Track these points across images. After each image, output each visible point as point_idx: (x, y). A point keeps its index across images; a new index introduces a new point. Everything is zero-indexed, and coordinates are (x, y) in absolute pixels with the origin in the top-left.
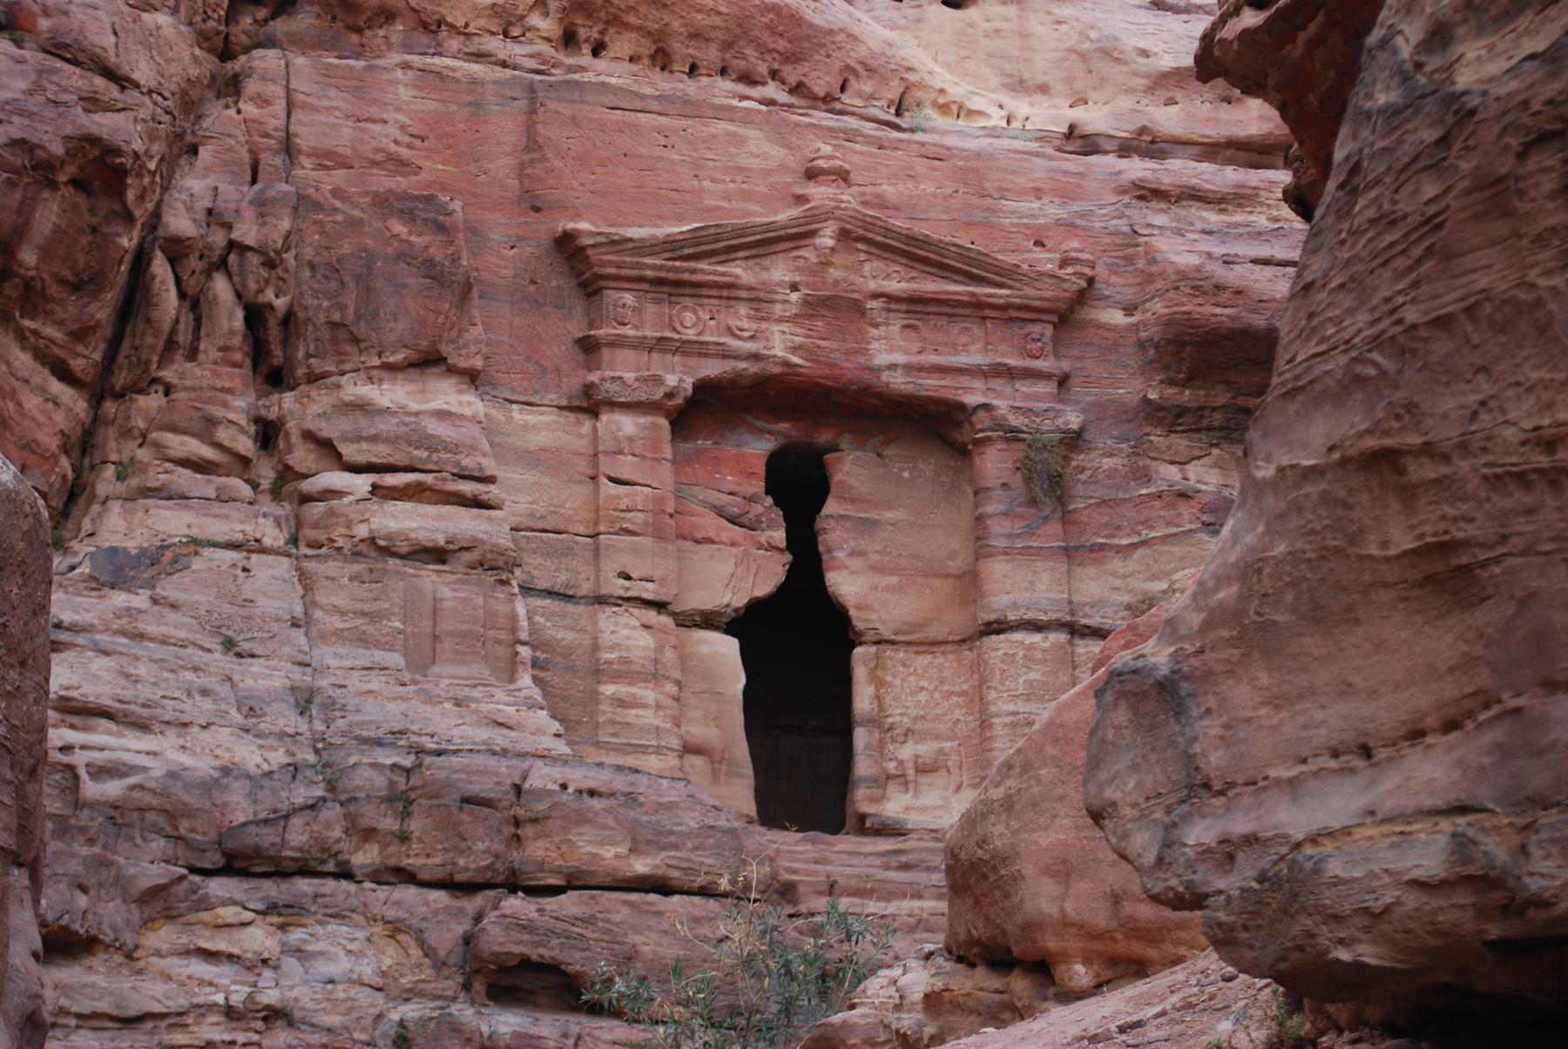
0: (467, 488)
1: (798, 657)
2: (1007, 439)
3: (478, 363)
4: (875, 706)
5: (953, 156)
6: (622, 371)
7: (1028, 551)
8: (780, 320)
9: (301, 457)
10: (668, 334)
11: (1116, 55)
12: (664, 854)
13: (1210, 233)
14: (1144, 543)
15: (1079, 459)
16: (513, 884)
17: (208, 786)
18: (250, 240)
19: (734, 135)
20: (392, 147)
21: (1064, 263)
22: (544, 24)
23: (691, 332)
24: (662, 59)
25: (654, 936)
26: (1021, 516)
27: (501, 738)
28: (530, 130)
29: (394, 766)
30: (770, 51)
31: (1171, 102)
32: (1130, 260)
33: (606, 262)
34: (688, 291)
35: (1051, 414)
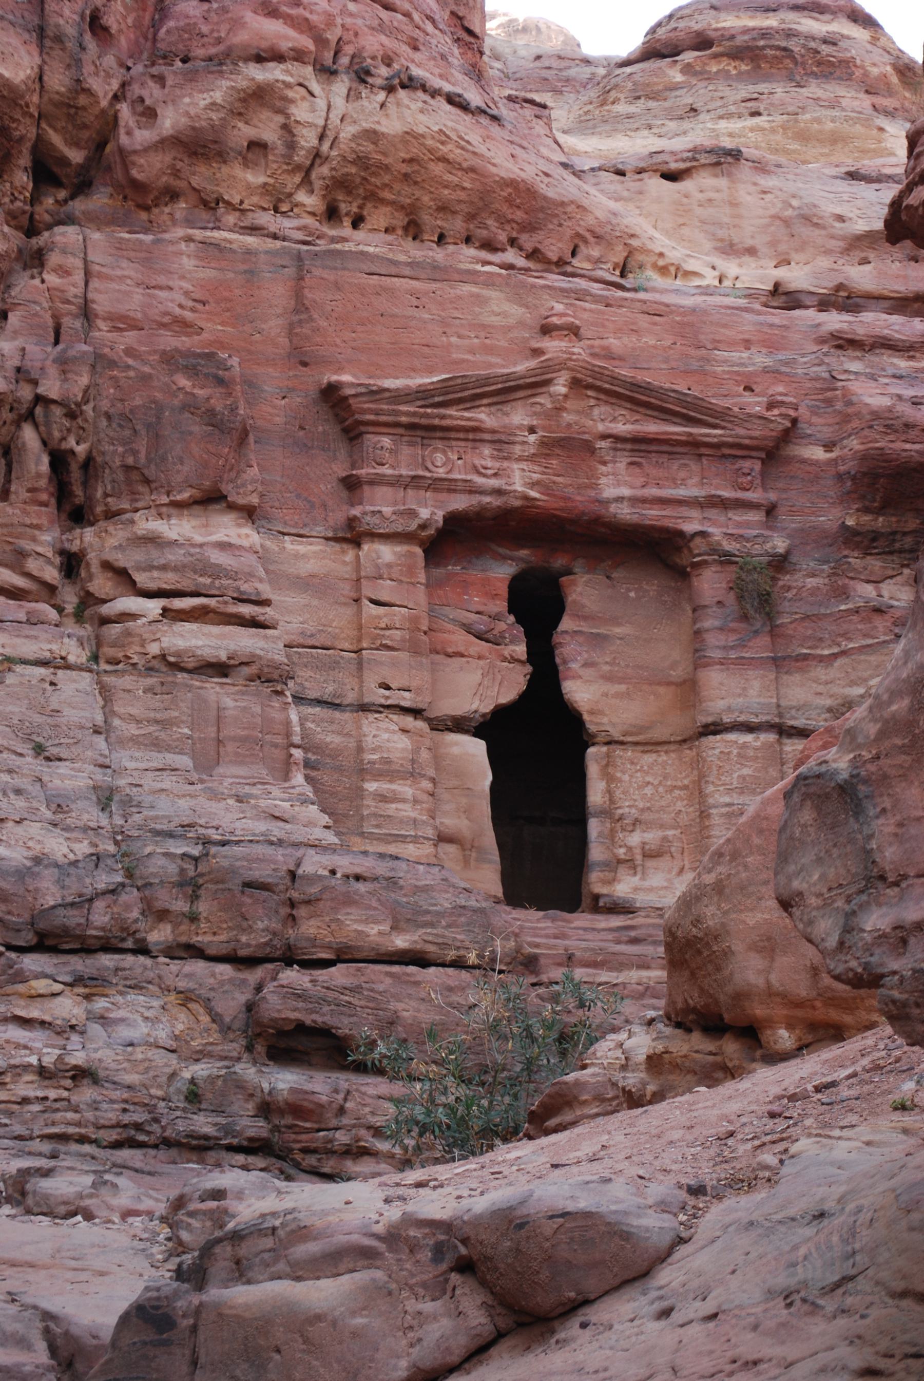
0: (246, 610)
1: (539, 759)
2: (721, 563)
3: (255, 500)
5: (672, 312)
6: (381, 506)
7: (741, 662)
8: (520, 459)
9: (100, 584)
10: (421, 473)
11: (815, 220)
13: (900, 377)
14: (843, 653)
15: (785, 579)
16: (290, 958)
17: (22, 874)
18: (54, 395)
19: (478, 296)
20: (178, 311)
21: (770, 406)
22: (309, 200)
23: (441, 470)
24: (414, 230)
25: (413, 1003)
26: (733, 631)
27: (277, 830)
28: (298, 295)
29: (184, 855)
30: (509, 222)
31: (865, 261)
32: (829, 402)
33: (366, 410)
34: (439, 434)
35: (760, 540)
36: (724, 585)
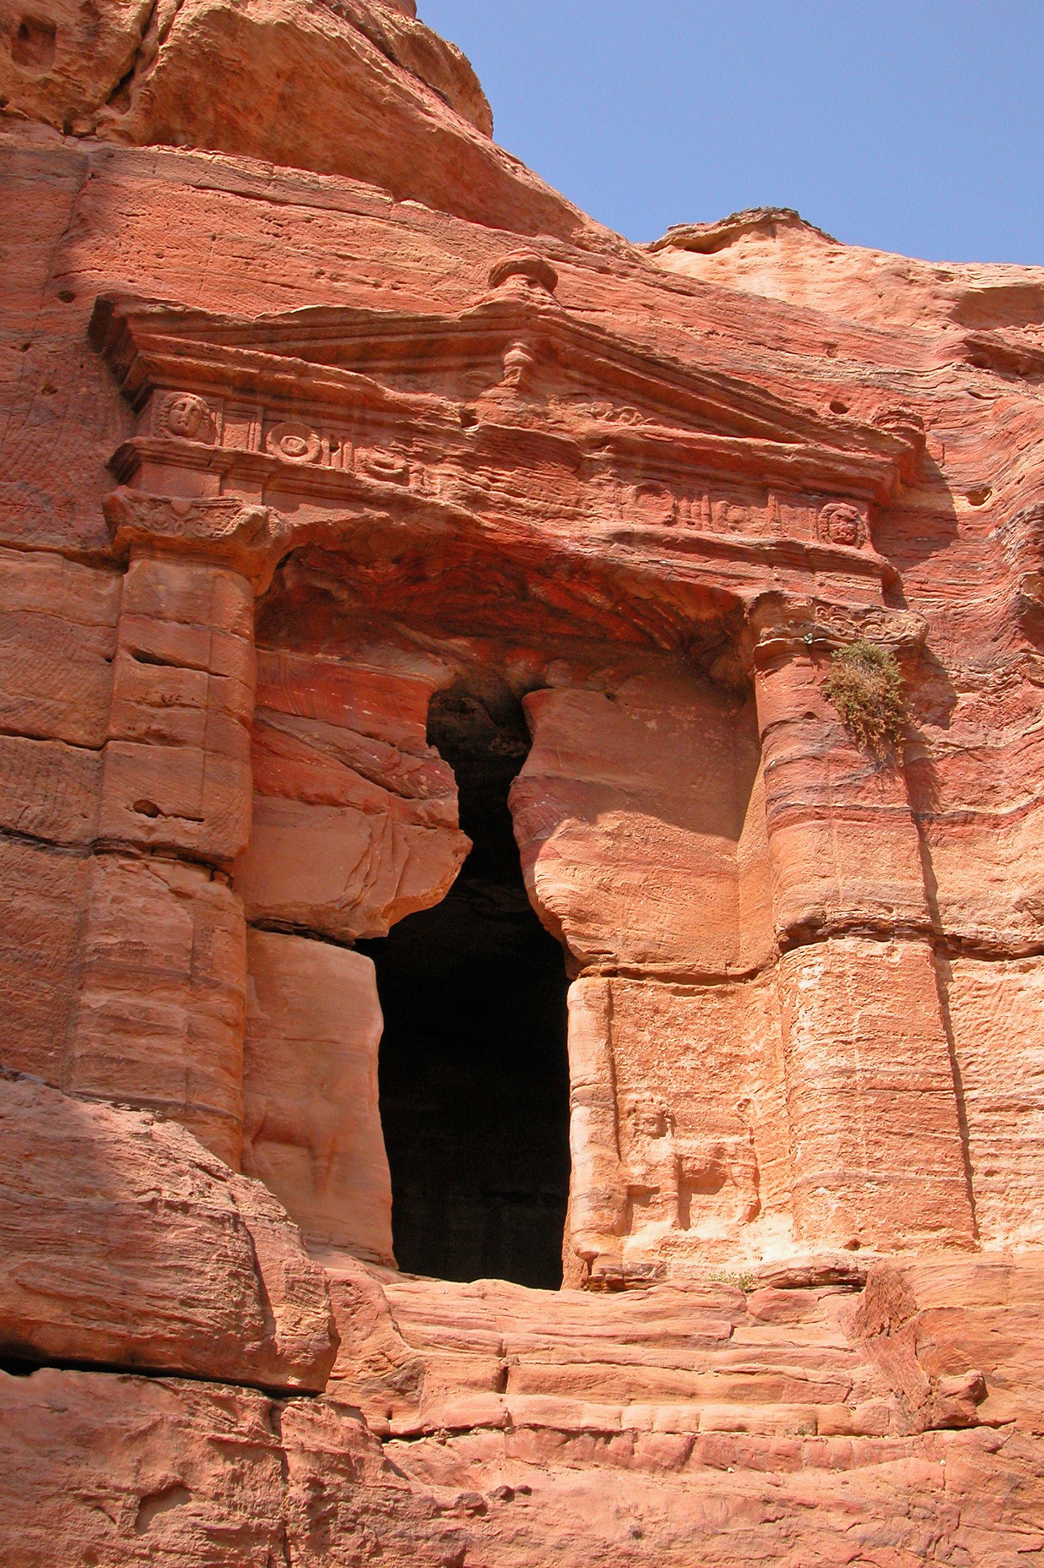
12: (20, 1259)
26: (838, 761)
33: (165, 350)
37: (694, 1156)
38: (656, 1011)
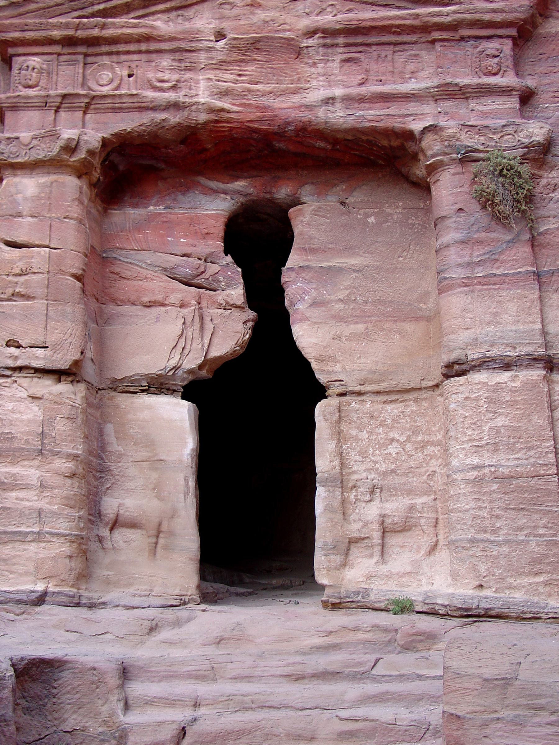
4: (336, 463)
7: (487, 281)
23: (106, 88)
26: (480, 242)
34: (105, 49)
35: (510, 129)
36: (466, 189)
37: (394, 514)
38: (372, 417)
